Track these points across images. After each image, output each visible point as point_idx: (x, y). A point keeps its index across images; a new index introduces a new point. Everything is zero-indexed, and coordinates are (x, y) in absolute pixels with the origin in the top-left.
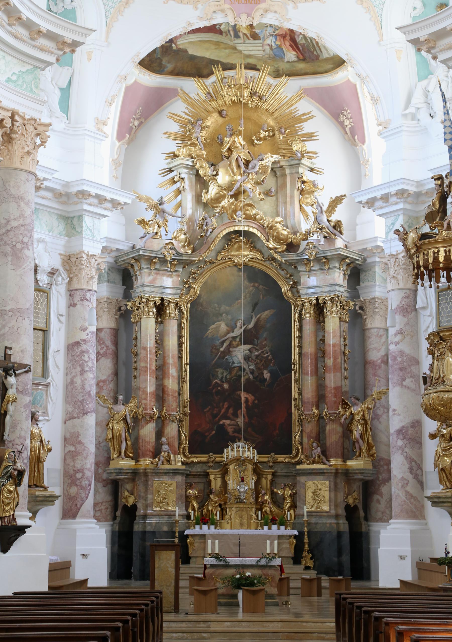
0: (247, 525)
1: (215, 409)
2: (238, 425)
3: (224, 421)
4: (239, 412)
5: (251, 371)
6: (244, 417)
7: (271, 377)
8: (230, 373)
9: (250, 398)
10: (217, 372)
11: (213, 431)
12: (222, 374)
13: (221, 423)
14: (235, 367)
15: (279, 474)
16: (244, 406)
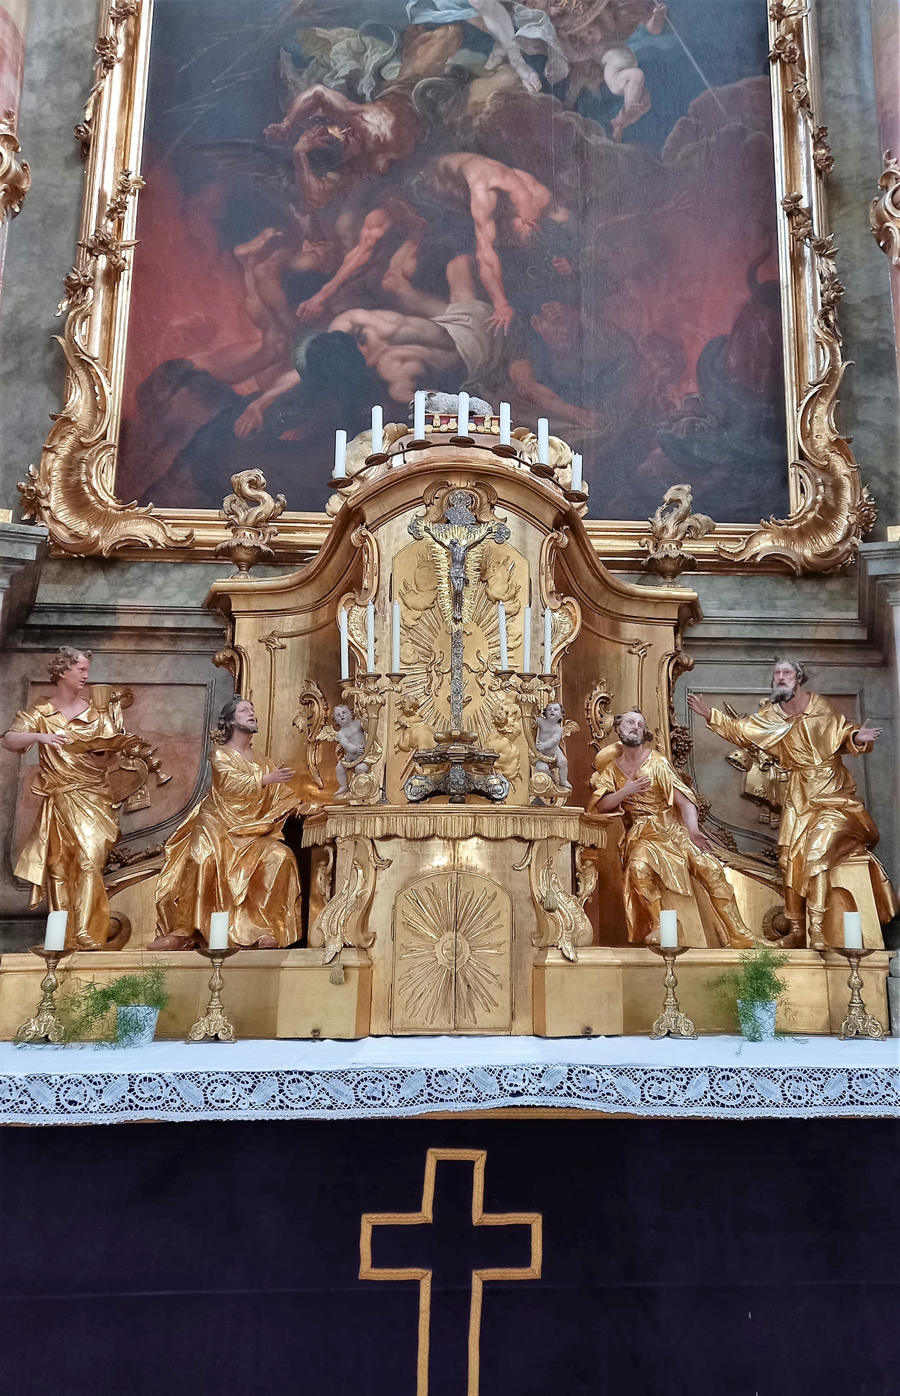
0: (503, 997)
1: (306, 246)
2: (448, 344)
3: (361, 316)
4: (457, 268)
5: (531, 51)
6: (481, 292)
7: (649, 86)
8: (404, 51)
9: (520, 196)
10: (327, 44)
11: (284, 369)
12: (358, 55)
13: (342, 324)
14: (431, 27)
15: (714, 632)
16: (486, 233)
